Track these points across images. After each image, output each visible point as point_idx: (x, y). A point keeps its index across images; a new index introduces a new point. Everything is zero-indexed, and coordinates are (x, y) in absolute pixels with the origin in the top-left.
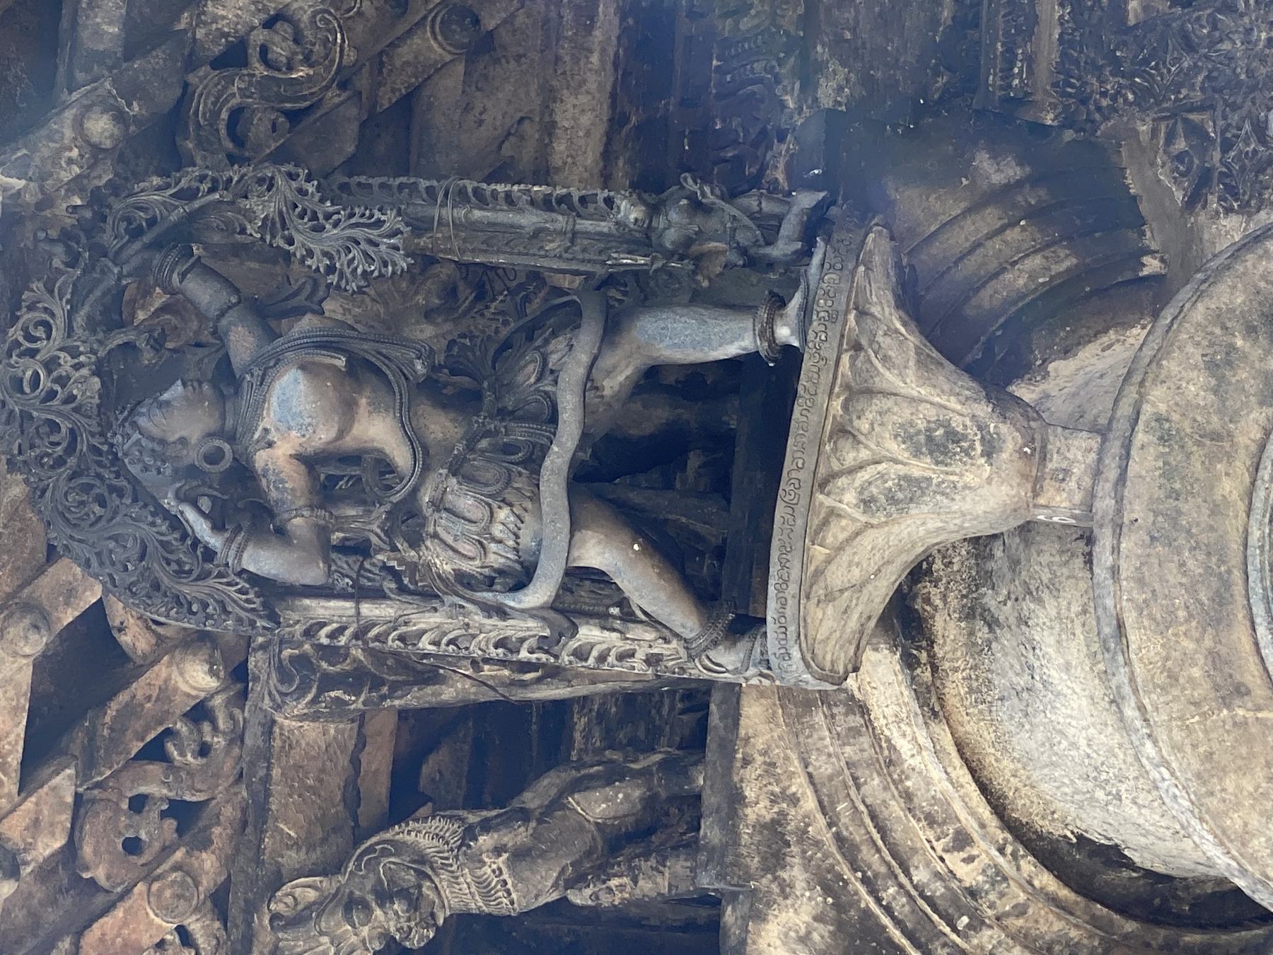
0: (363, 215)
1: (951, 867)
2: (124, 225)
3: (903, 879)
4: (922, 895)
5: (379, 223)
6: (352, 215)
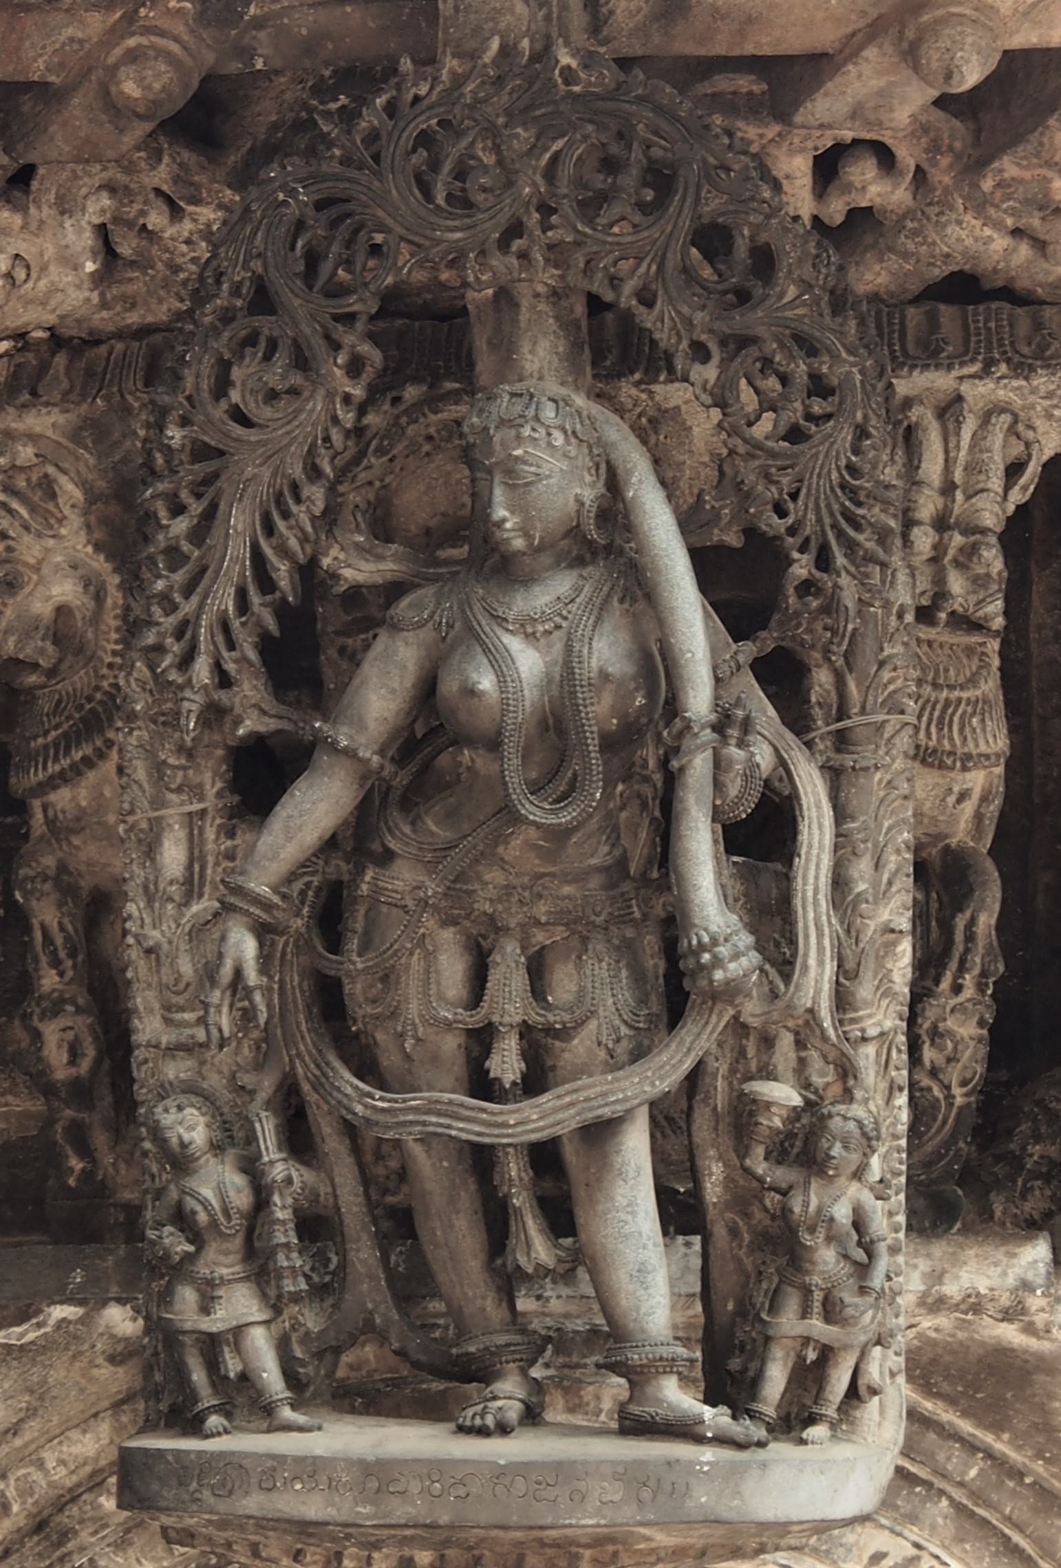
1: (899, 1539)
3: (959, 1495)
4: (928, 1485)
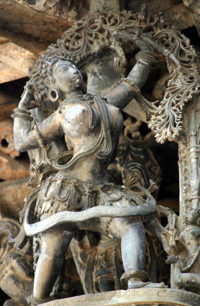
0: (178, 118)
2: (164, 35)
5: (175, 125)
6: (178, 115)
